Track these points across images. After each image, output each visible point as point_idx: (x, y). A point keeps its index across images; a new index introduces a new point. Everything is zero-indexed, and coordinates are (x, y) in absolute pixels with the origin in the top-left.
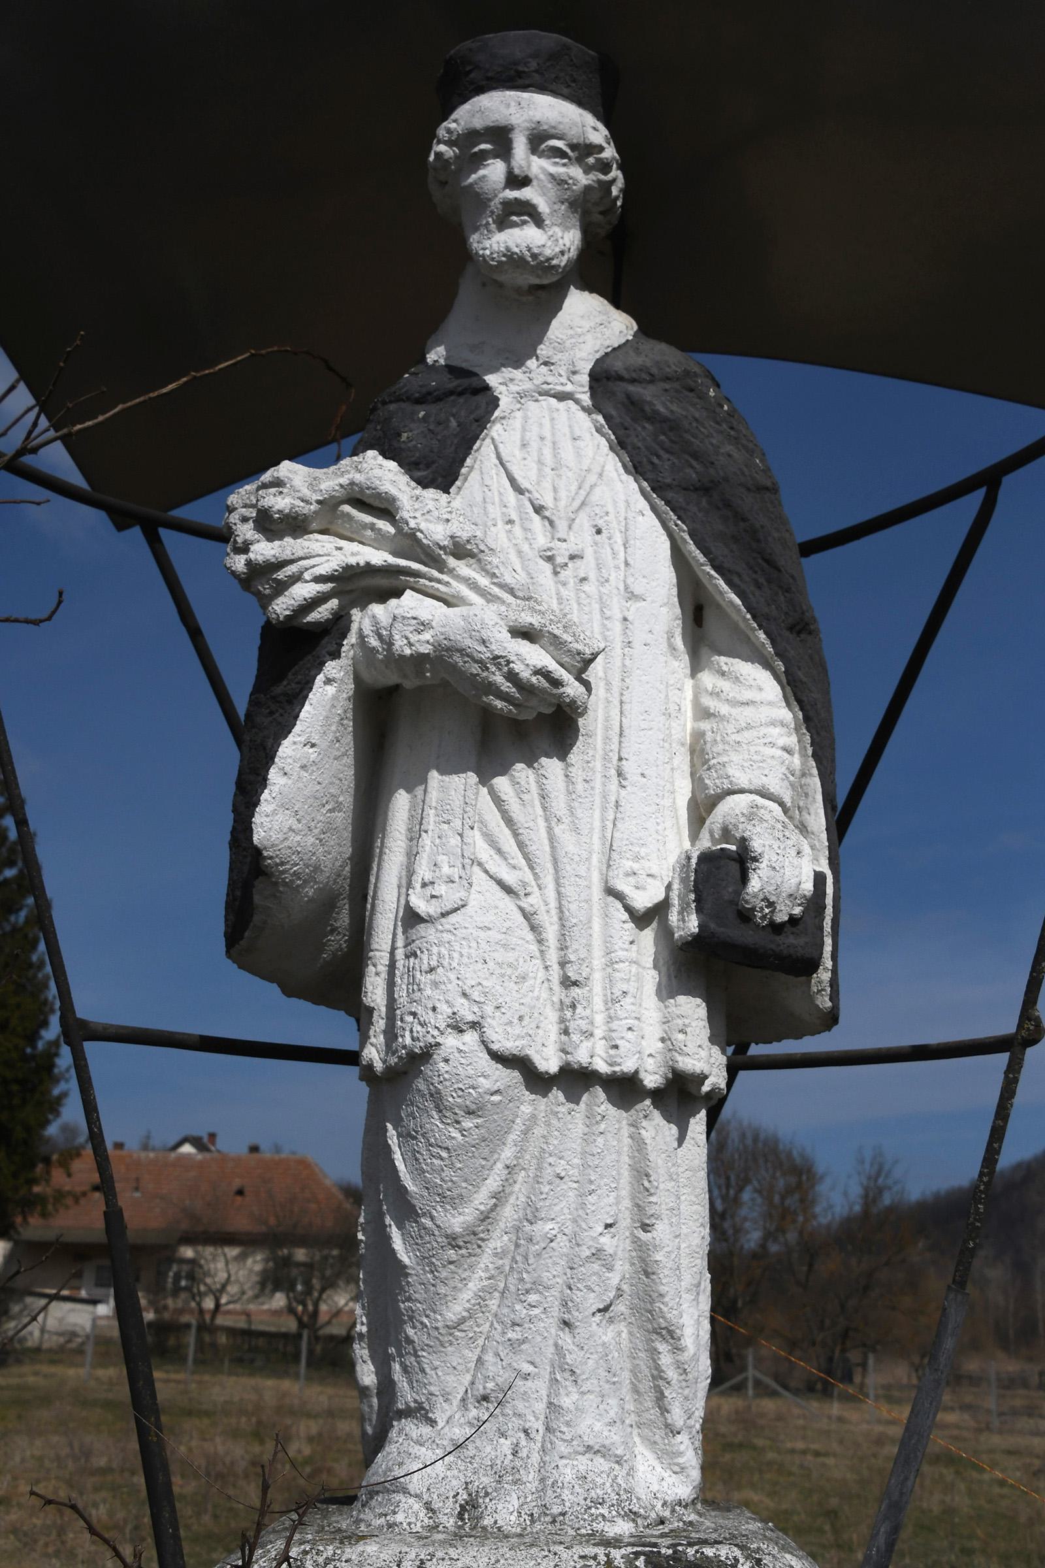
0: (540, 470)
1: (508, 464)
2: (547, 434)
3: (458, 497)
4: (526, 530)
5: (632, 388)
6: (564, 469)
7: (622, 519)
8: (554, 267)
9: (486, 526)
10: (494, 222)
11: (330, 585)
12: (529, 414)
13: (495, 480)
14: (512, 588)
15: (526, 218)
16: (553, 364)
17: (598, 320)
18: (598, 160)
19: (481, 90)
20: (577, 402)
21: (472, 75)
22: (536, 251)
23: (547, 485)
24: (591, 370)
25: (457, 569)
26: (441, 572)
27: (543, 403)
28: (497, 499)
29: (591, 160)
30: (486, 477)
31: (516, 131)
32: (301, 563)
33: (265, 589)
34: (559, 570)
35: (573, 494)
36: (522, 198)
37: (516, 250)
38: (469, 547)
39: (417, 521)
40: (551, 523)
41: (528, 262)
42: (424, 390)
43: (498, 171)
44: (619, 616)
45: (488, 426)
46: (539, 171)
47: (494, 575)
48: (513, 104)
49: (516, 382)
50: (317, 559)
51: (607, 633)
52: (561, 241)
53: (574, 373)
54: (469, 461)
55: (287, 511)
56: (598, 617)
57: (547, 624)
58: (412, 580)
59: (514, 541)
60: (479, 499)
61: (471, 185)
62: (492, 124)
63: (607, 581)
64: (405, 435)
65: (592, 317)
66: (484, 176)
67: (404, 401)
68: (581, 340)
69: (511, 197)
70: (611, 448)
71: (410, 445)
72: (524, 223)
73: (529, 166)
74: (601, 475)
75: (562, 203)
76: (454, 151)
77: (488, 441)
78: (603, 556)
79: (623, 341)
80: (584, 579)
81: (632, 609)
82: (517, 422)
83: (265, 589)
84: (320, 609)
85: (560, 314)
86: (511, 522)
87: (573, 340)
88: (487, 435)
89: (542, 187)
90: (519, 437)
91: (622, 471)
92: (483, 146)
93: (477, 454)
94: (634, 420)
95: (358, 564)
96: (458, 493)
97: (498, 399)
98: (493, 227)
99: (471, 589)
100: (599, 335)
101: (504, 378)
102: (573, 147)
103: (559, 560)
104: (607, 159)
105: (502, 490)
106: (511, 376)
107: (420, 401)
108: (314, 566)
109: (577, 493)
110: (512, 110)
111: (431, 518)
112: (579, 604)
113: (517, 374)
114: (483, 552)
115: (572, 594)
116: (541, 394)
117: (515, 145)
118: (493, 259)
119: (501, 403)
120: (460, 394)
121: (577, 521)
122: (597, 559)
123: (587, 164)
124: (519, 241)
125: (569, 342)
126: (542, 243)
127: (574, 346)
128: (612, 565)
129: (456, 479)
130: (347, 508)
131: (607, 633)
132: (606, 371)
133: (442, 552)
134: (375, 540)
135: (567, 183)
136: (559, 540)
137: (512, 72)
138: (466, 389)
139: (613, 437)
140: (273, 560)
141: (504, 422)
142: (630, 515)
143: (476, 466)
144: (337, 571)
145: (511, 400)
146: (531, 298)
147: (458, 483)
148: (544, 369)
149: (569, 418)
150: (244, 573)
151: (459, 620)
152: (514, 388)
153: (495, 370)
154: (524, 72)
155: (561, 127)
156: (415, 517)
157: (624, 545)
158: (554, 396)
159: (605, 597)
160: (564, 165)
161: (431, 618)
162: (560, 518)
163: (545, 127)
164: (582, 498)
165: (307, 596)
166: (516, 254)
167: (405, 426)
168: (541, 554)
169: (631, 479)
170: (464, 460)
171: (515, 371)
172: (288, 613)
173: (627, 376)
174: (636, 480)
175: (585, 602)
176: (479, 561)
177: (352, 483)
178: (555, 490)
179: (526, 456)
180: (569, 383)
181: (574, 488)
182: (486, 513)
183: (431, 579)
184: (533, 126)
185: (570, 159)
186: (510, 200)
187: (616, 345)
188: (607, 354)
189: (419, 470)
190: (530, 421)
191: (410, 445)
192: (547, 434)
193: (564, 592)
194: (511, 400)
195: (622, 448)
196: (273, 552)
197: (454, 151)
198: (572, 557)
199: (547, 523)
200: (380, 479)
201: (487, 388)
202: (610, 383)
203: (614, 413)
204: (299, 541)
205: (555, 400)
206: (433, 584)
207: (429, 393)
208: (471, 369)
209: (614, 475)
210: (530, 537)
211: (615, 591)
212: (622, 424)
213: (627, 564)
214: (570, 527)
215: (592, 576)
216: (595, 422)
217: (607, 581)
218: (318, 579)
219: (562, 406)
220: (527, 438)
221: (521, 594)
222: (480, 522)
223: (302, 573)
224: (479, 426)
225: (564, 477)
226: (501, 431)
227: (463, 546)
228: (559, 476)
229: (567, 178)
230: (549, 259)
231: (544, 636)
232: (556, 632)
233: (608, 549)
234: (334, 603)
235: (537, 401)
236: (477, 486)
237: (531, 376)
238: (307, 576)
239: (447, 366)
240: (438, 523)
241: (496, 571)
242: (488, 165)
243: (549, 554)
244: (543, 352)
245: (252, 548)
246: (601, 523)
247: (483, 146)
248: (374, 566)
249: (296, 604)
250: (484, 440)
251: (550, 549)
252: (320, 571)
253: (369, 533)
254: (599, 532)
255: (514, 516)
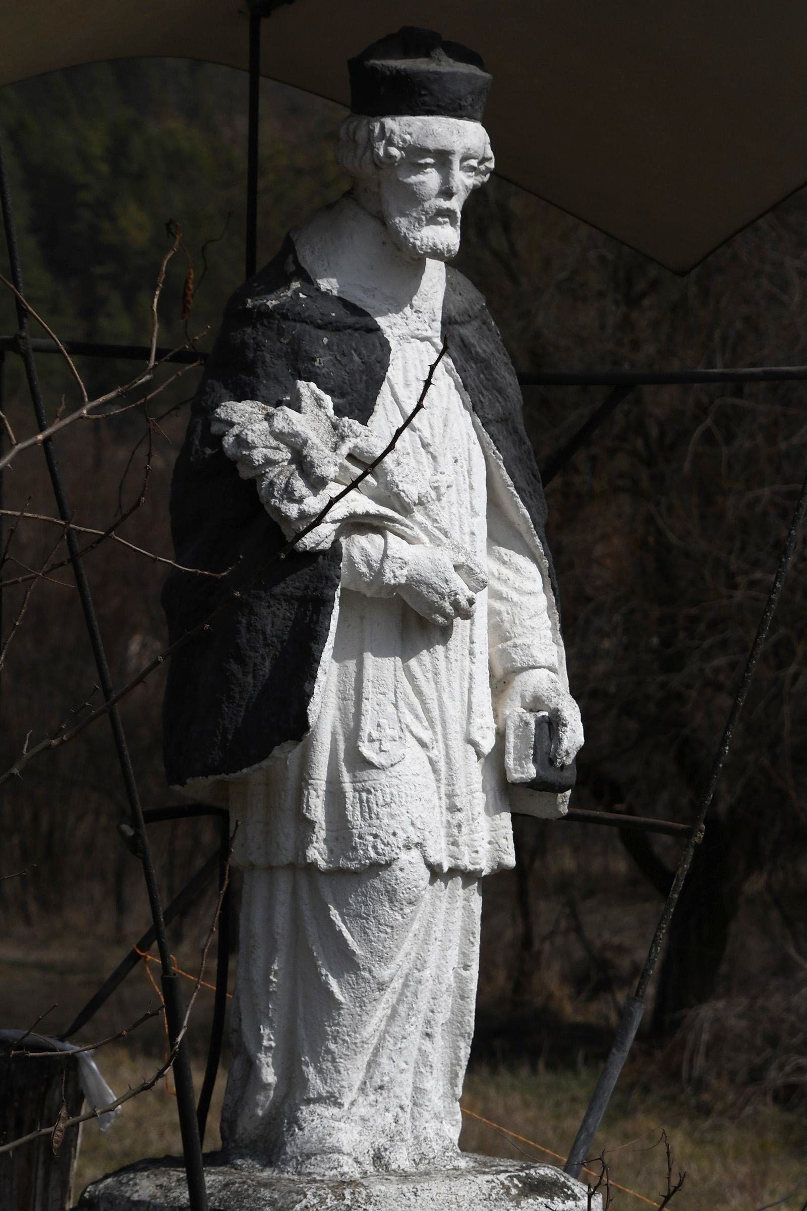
7: (466, 449)
16: (421, 312)
37: (440, 247)
40: (434, 458)
46: (460, 183)
47: (435, 521)
49: (398, 326)
58: (391, 524)
66: (424, 182)
70: (456, 388)
72: (445, 223)
101: (390, 322)
110: (455, 138)
111: (408, 480)
116: (412, 337)
118: (421, 249)
120: (356, 330)
124: (443, 240)
138: (362, 327)
139: (460, 380)
151: (428, 561)
153: (384, 313)
158: (419, 339)
166: (440, 250)
169: (468, 413)
176: (426, 508)
178: (431, 427)
184: (465, 151)
195: (466, 390)
197: (402, 154)
199: (430, 457)
206: (403, 528)
207: (331, 323)
208: (363, 308)
236: (383, 421)
237: (407, 322)
241: (437, 518)
242: (427, 173)
243: (436, 485)
245: (305, 501)
254: (456, 461)
255: (410, 451)
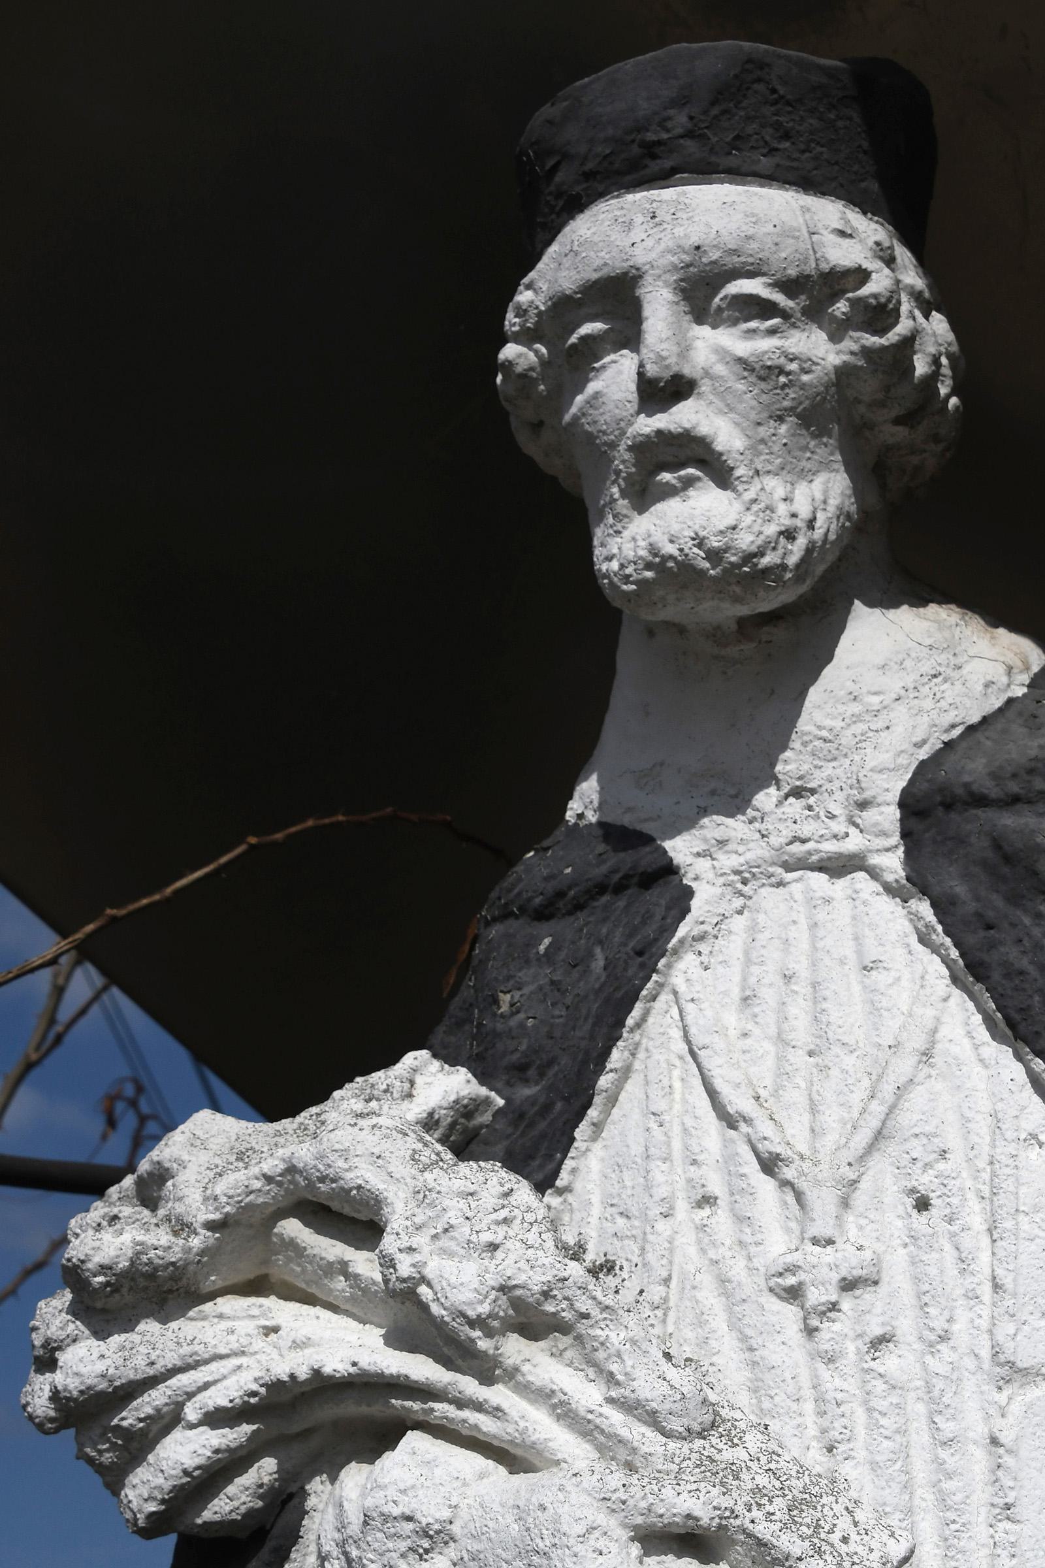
0: (780, 1058)
1: (702, 1054)
2: (800, 966)
3: (597, 1147)
4: (742, 1220)
5: (1008, 821)
6: (836, 1049)
7: (982, 1163)
8: (767, 571)
9: (645, 1218)
10: (624, 494)
11: (247, 1429)
12: (761, 918)
13: (677, 1096)
14: (655, 1412)
15: (691, 471)
16: (813, 791)
17: (927, 667)
18: (854, 303)
19: (576, 205)
20: (874, 873)
21: (559, 177)
22: (715, 543)
23: (795, 1095)
24: (904, 792)
25: (526, 1368)
26: (487, 1379)
27: (796, 888)
28: (677, 1145)
29: (841, 307)
30: (654, 1091)
31: (648, 279)
32: (173, 1382)
33: (100, 1452)
34: (815, 1322)
35: (856, 1115)
36: (673, 428)
37: (670, 549)
38: (550, 1308)
39: (417, 1257)
40: (799, 1196)
41: (702, 573)
42: (550, 887)
43: (625, 376)
44: (980, 1431)
45: (661, 963)
46: (713, 358)
47: (611, 1379)
48: (639, 219)
49: (730, 847)
50: (213, 1366)
51: (947, 1485)
52: (782, 509)
53: (863, 805)
54: (617, 1057)
55: (124, 1264)
56: (926, 1438)
57: (740, 1509)
58: (416, 1406)
59: (712, 1254)
60: (637, 1149)
61: (576, 419)
62: (595, 276)
63: (825, 1413)
64: (505, 999)
65: (908, 663)
66: (597, 395)
67: (517, 917)
68: (879, 724)
69: (647, 430)
70: (955, 980)
71: (513, 1022)
72: (689, 483)
73: (685, 351)
74: (927, 1055)
75: (780, 419)
76: (536, 352)
77: (665, 997)
78: (933, 1271)
79: (998, 703)
80: (881, 1342)
81: (1015, 1408)
82: (732, 946)
83: (100, 1452)
84: (231, 1489)
85: (828, 672)
86: (707, 1200)
87: (860, 728)
88: (661, 985)
89: (723, 393)
90: (737, 978)
91: (983, 1034)
92: (587, 329)
93: (637, 1036)
94: (1014, 899)
95: (292, 1376)
96: (595, 1138)
97: (688, 893)
98: (623, 505)
99: (559, 1418)
100: (928, 704)
101: (705, 840)
102: (789, 286)
103: (815, 1296)
104: (875, 296)
105: (690, 1123)
106: (719, 833)
107: (543, 914)
108: (206, 1386)
109: (864, 1111)
110: (637, 234)
111: (452, 1245)
112: (870, 1410)
113: (735, 827)
114: (586, 1316)
115: (852, 1386)
116: (788, 867)
117: (647, 311)
118: (627, 579)
119: (695, 903)
120: (619, 889)
121: (863, 1185)
122: (917, 1280)
123: (833, 318)
124: (675, 528)
125: (849, 733)
126: (730, 521)
127: (863, 738)
128: (959, 1291)
129: (588, 1104)
130: (292, 1228)
131: (947, 1485)
132: (941, 790)
133: (477, 1333)
134: (353, 1299)
135: (781, 371)
136: (815, 1241)
137: (636, 150)
138: (627, 877)
139: (954, 953)
140: (103, 1386)
141: (703, 947)
142: (1003, 1151)
143: (637, 1065)
144: (254, 1394)
145: (719, 891)
146: (748, 647)
147: (593, 1113)
148: (794, 806)
149: (854, 918)
150: (52, 1420)
151: (510, 1519)
152: (728, 862)
153: (684, 823)
154: (660, 143)
155: (754, 246)
156: (411, 1250)
157: (990, 1231)
158: (820, 868)
159: (939, 1384)
160: (772, 332)
161: (446, 1514)
162: (817, 1183)
163: (715, 255)
164: (875, 1123)
165: (190, 1462)
166: (671, 557)
167: (509, 978)
168: (772, 1283)
169: (1005, 1054)
170: (606, 1053)
171: (729, 821)
172: (152, 1507)
173: (994, 792)
174: (1019, 1057)
175: (882, 1405)
176: (579, 1338)
177: (291, 1170)
178: (814, 1109)
179: (750, 1026)
180: (852, 830)
181: (858, 1096)
182: (648, 1188)
183: (460, 1403)
184: (687, 258)
185: (785, 315)
186: (648, 436)
187: (975, 719)
188: (948, 745)
189: (526, 1081)
190: (762, 938)
191: (513, 1022)
192: (800, 966)
193: (831, 1381)
194: (719, 891)
195: (978, 979)
196: (100, 1367)
197: (536, 352)
198: (848, 1285)
199: (790, 1198)
200: (344, 1154)
201: (669, 870)
202: (953, 816)
203: (960, 890)
204: (174, 1325)
205: (823, 877)
206: (466, 1414)
207: (560, 894)
208: (639, 827)
209: (963, 1049)
210: (748, 1239)
211: (970, 1363)
212: (979, 915)
213: (997, 1287)
214: (845, 1203)
215: (906, 1326)
216: (915, 917)
217: (944, 1338)
218: (216, 1418)
219: (842, 883)
220: (752, 980)
221: (676, 1425)
222: (634, 1211)
223: (180, 1406)
224: (642, 966)
225: (835, 1072)
226: (696, 972)
227: (535, 1308)
228: (824, 1069)
229: (782, 360)
230: (749, 557)
231: (734, 1542)
232: (763, 1530)
233: (948, 1247)
235: (781, 884)
236: (636, 1116)
237: (763, 827)
238: (191, 1413)
239: (600, 824)
240: (468, 1258)
241: (614, 1368)
242: (603, 367)
243: (791, 1281)
244: (788, 768)
245: (63, 1358)
246: (925, 1181)
247: (587, 329)
248: (331, 1377)
249: (168, 1485)
250: (654, 998)
251: (792, 1269)
252: (218, 1398)
253: (340, 1283)
254: (923, 1204)
255: (716, 1186)
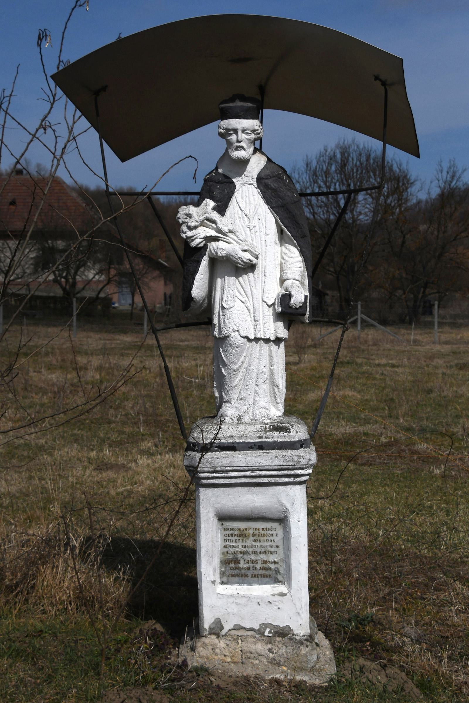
4: (244, 220)
5: (266, 181)
23: (248, 208)
82: (240, 191)
94: (267, 190)
97: (236, 186)
103: (251, 228)
113: (240, 179)
130: (206, 221)
153: (235, 178)
192: (247, 195)
193: (252, 235)
201: (233, 182)
218: (201, 239)
234: (204, 242)
246: (260, 217)
